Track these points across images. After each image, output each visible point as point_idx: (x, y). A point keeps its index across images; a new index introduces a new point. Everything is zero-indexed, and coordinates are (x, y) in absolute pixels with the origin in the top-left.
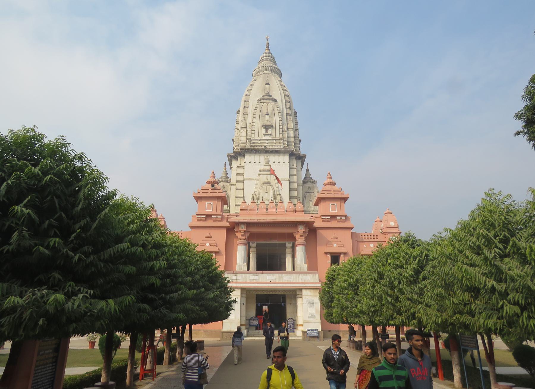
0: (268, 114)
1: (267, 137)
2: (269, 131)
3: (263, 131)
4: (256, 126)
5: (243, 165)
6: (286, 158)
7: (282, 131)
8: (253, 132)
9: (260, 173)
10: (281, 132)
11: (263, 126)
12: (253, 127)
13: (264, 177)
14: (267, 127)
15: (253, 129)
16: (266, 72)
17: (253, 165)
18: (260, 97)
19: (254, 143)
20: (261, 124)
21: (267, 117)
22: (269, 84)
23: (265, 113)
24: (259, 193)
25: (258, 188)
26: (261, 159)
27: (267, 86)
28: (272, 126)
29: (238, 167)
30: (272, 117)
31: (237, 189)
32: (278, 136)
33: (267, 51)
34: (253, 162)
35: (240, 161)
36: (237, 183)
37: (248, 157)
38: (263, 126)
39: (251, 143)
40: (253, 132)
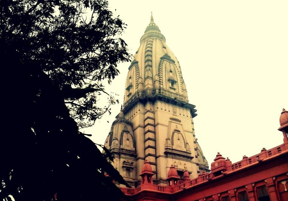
0: (171, 72)
1: (172, 91)
2: (175, 86)
3: (170, 85)
4: (164, 78)
5: (152, 110)
6: (188, 113)
7: (183, 89)
8: (162, 83)
9: (170, 120)
10: (182, 90)
11: (169, 80)
12: (161, 79)
13: (174, 126)
14: (173, 82)
15: (161, 81)
16: (159, 38)
17: (163, 112)
18: (162, 56)
19: (163, 93)
20: (167, 78)
21: (171, 74)
22: (165, 48)
23: (168, 69)
24: (172, 139)
25: (171, 134)
26: (169, 108)
27: (164, 49)
28: (176, 82)
29: (148, 111)
30: (175, 76)
31: (149, 131)
32: (181, 93)
33: (152, 22)
34: (164, 109)
35: (148, 107)
36: (149, 126)
37: (160, 105)
38: (169, 80)
39: (160, 92)
40: (162, 83)
